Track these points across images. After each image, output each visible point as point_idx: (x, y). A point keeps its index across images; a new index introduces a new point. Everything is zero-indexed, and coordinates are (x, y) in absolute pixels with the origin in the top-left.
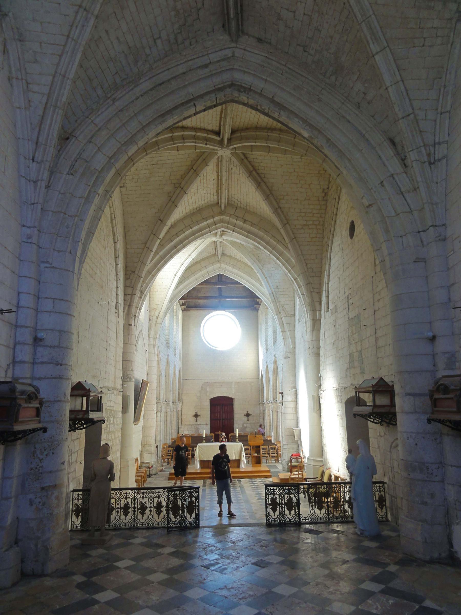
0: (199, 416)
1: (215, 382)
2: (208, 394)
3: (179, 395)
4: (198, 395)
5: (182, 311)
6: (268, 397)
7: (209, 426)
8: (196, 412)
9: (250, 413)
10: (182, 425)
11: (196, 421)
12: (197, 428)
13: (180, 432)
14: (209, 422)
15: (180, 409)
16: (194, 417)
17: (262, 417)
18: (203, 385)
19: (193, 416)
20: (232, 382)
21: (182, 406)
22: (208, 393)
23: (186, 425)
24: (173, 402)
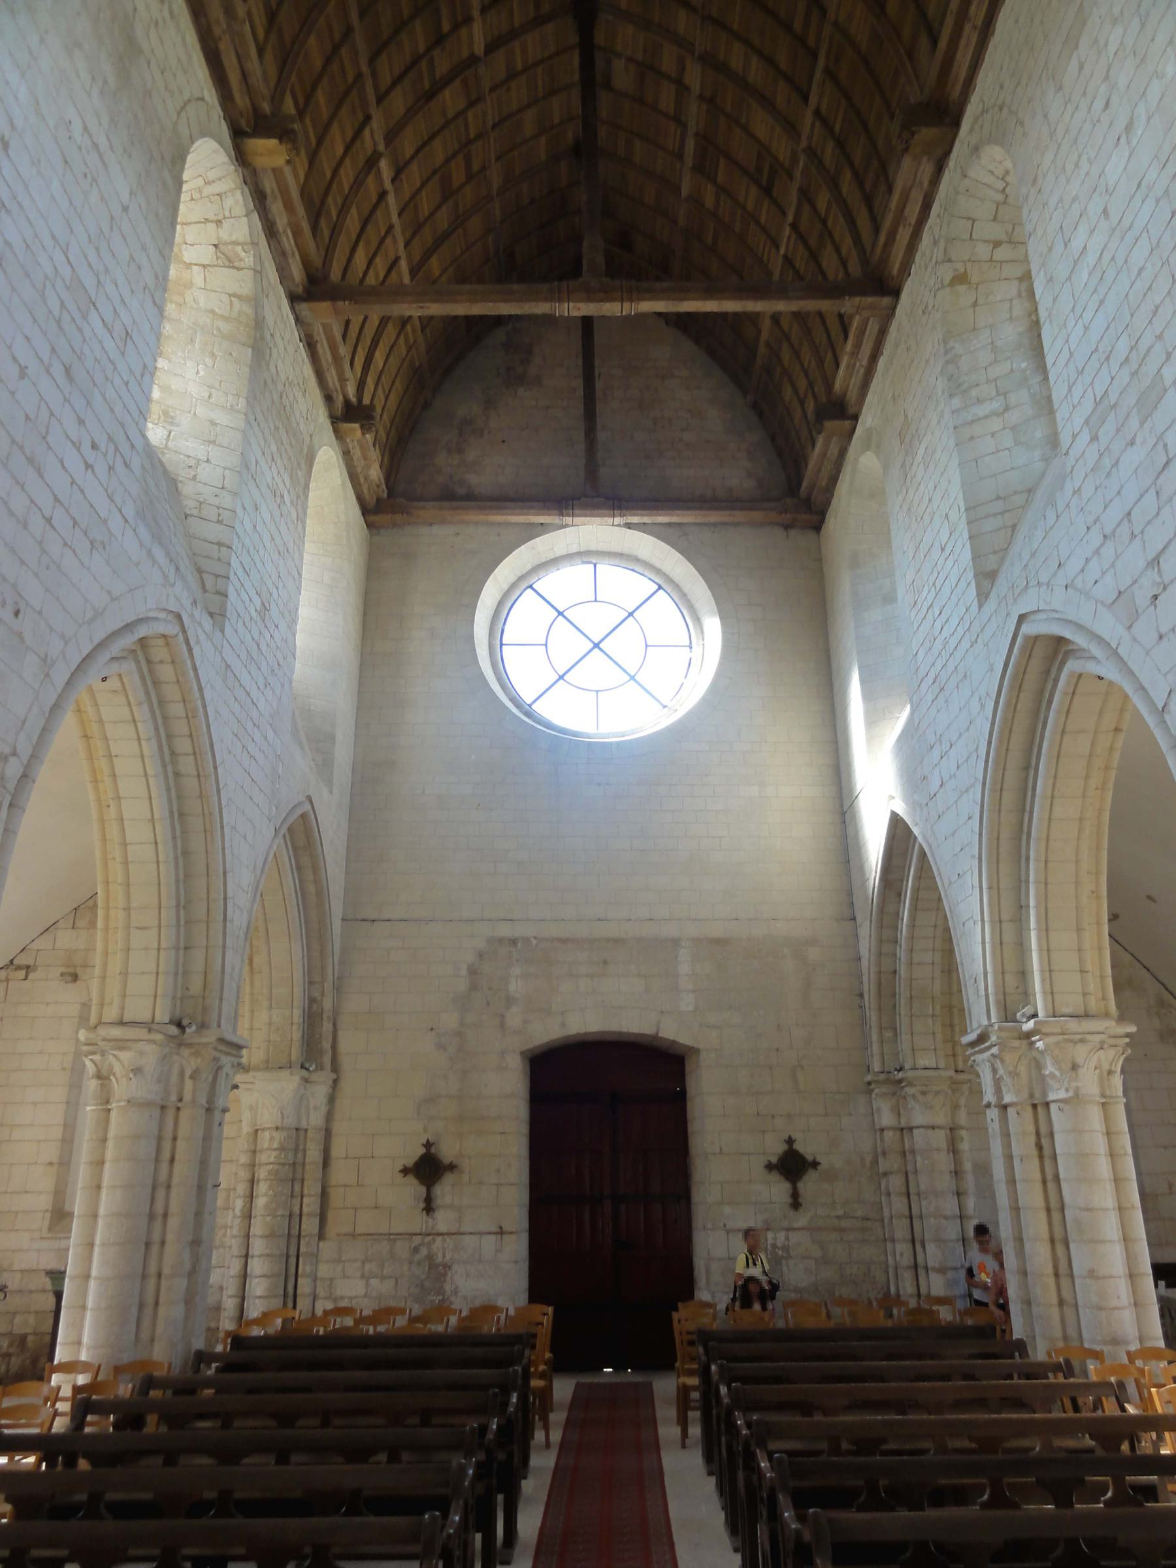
0: (452, 1167)
1: (564, 941)
2: (514, 1018)
3: (312, 1016)
4: (450, 1020)
5: (365, 511)
6: (1011, 981)
7: (517, 1247)
8: (428, 1145)
9: (807, 1148)
10: (321, 1236)
11: (429, 1207)
12: (430, 1258)
13: (304, 1286)
14: (516, 1214)
15: (316, 1119)
16: (411, 1180)
17: (896, 1182)
18: (481, 955)
19: (405, 1171)
20: (676, 942)
21: (332, 1100)
22: (515, 1010)
23: (353, 1235)
24: (179, 1025)
